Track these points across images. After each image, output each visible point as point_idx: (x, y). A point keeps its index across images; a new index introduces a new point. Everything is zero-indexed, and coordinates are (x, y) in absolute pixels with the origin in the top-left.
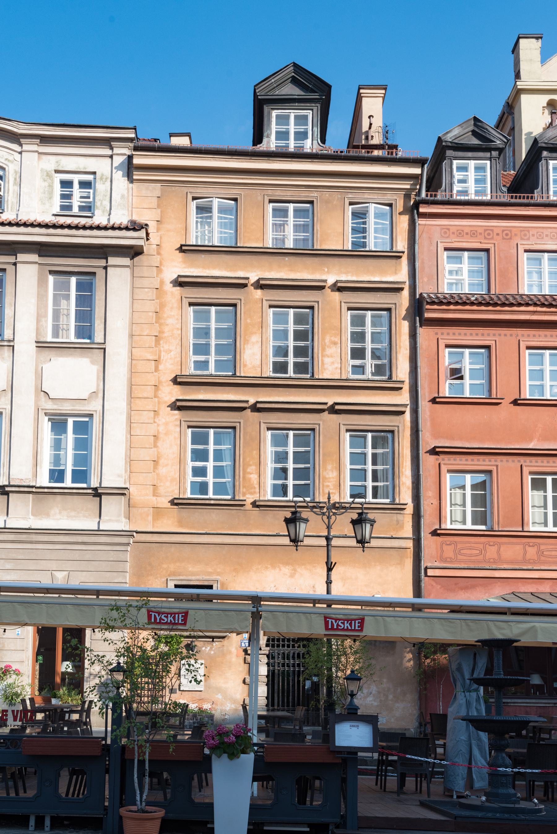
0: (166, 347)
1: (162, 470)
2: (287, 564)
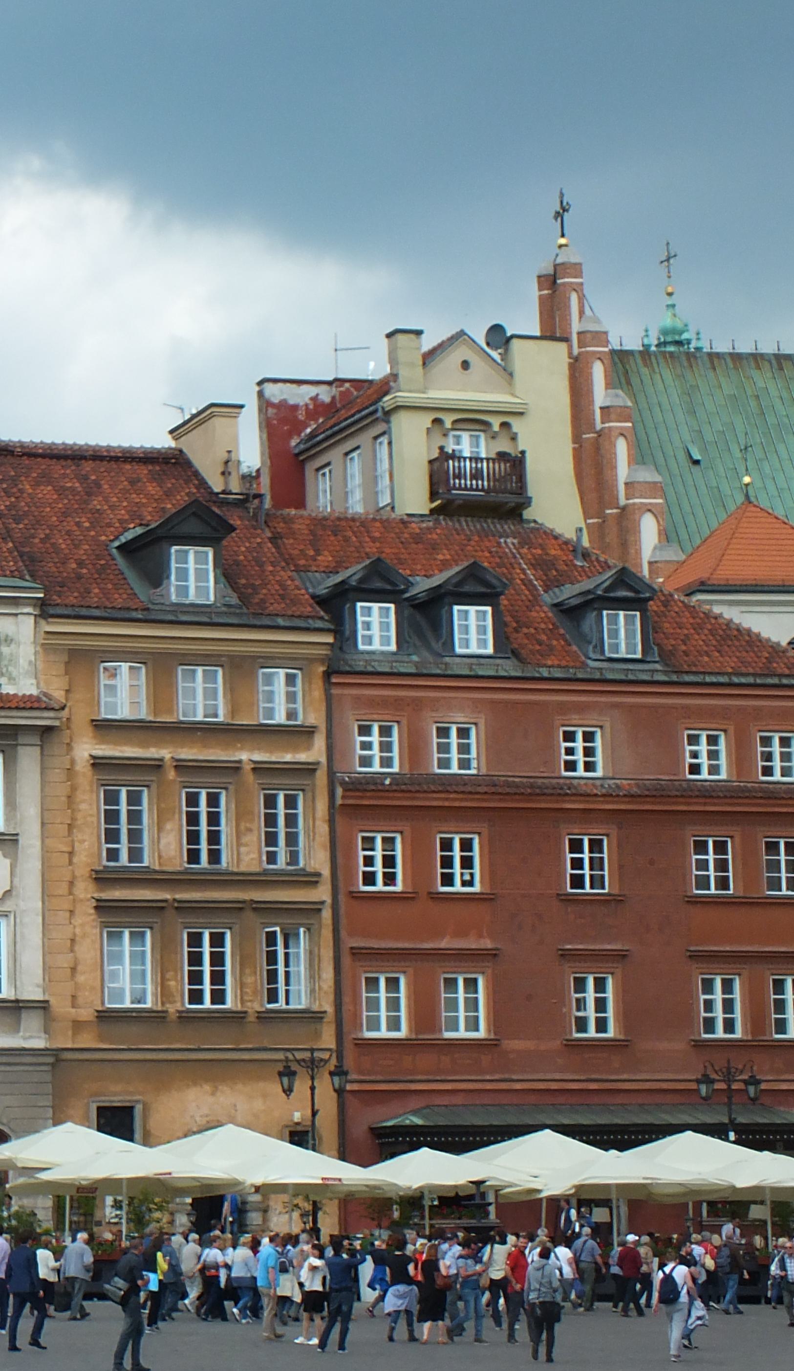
0: (80, 837)
1: (81, 978)
2: (207, 1081)
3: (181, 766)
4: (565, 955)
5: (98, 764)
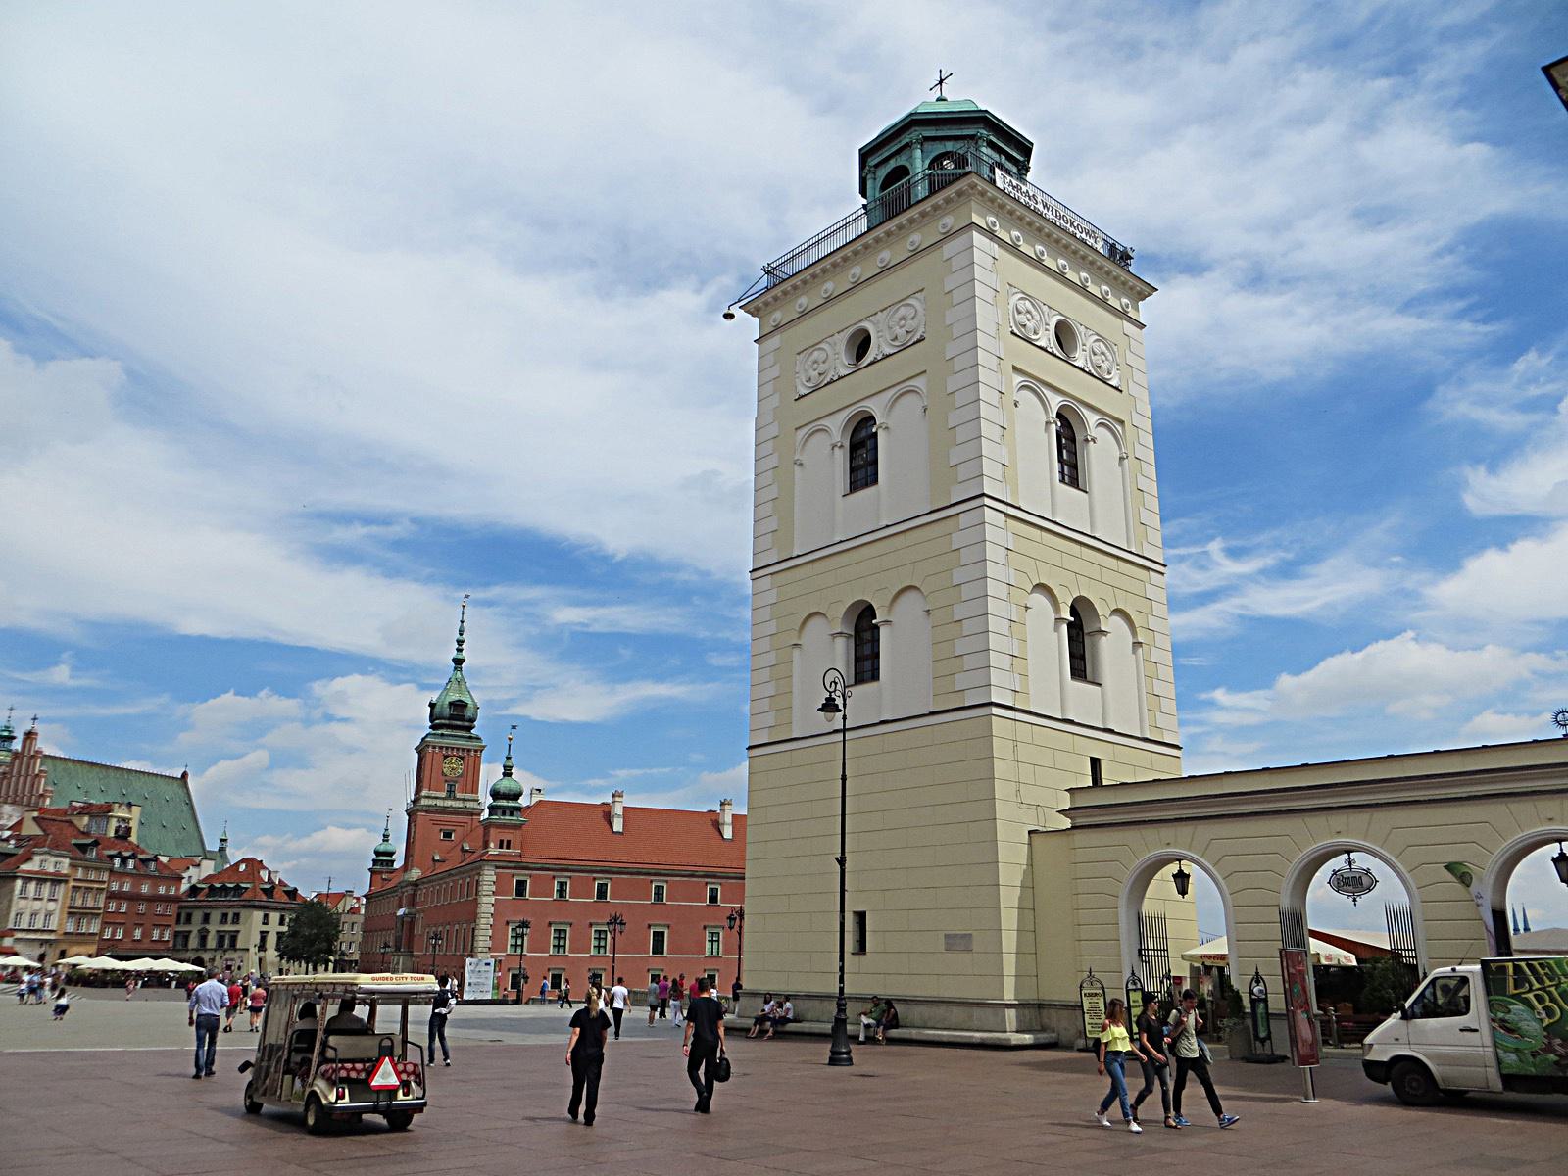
3: (87, 888)
4: (136, 924)
5: (74, 887)
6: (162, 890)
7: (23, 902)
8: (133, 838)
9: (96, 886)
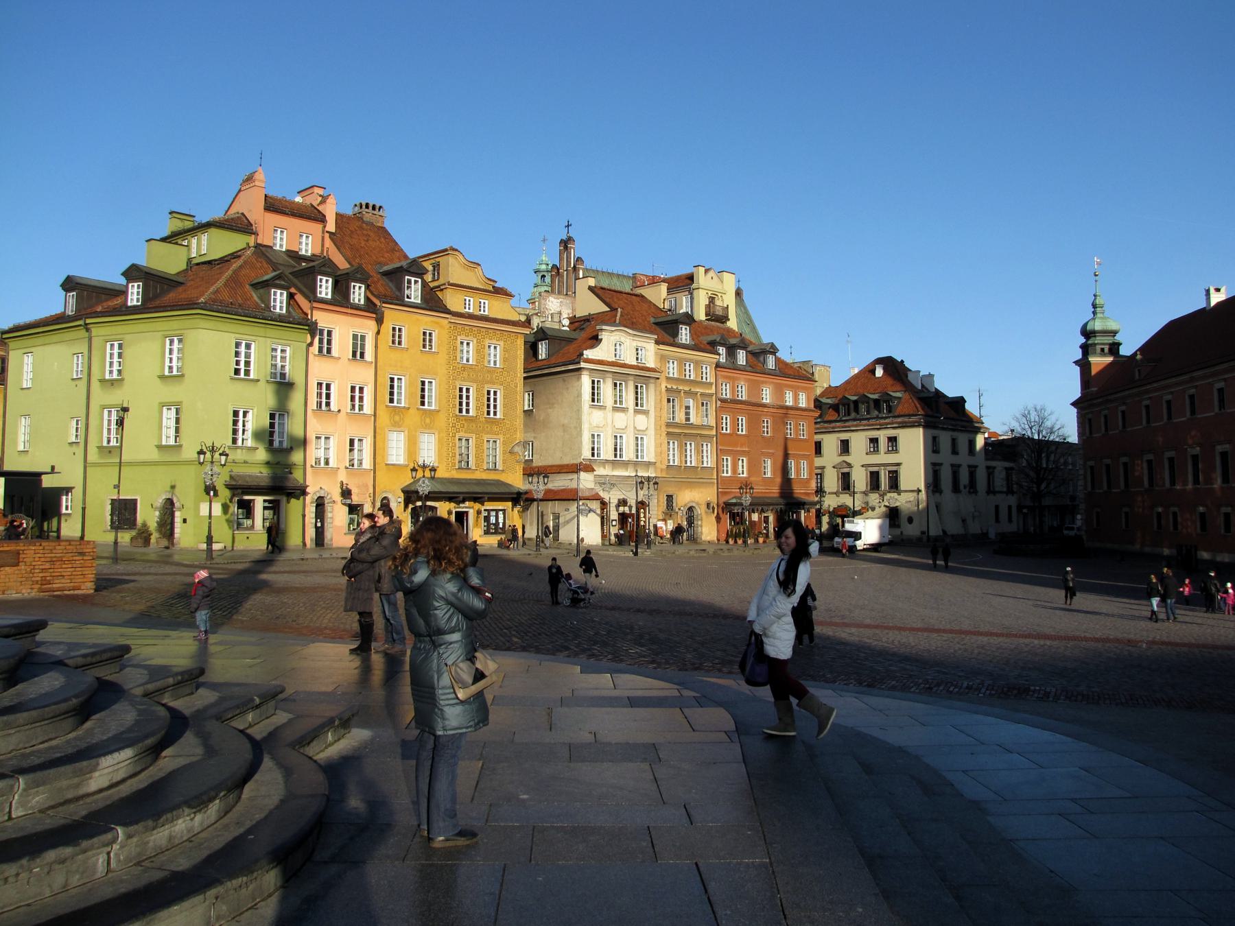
6: (789, 402)
7: (597, 416)
8: (732, 324)
9: (700, 390)
